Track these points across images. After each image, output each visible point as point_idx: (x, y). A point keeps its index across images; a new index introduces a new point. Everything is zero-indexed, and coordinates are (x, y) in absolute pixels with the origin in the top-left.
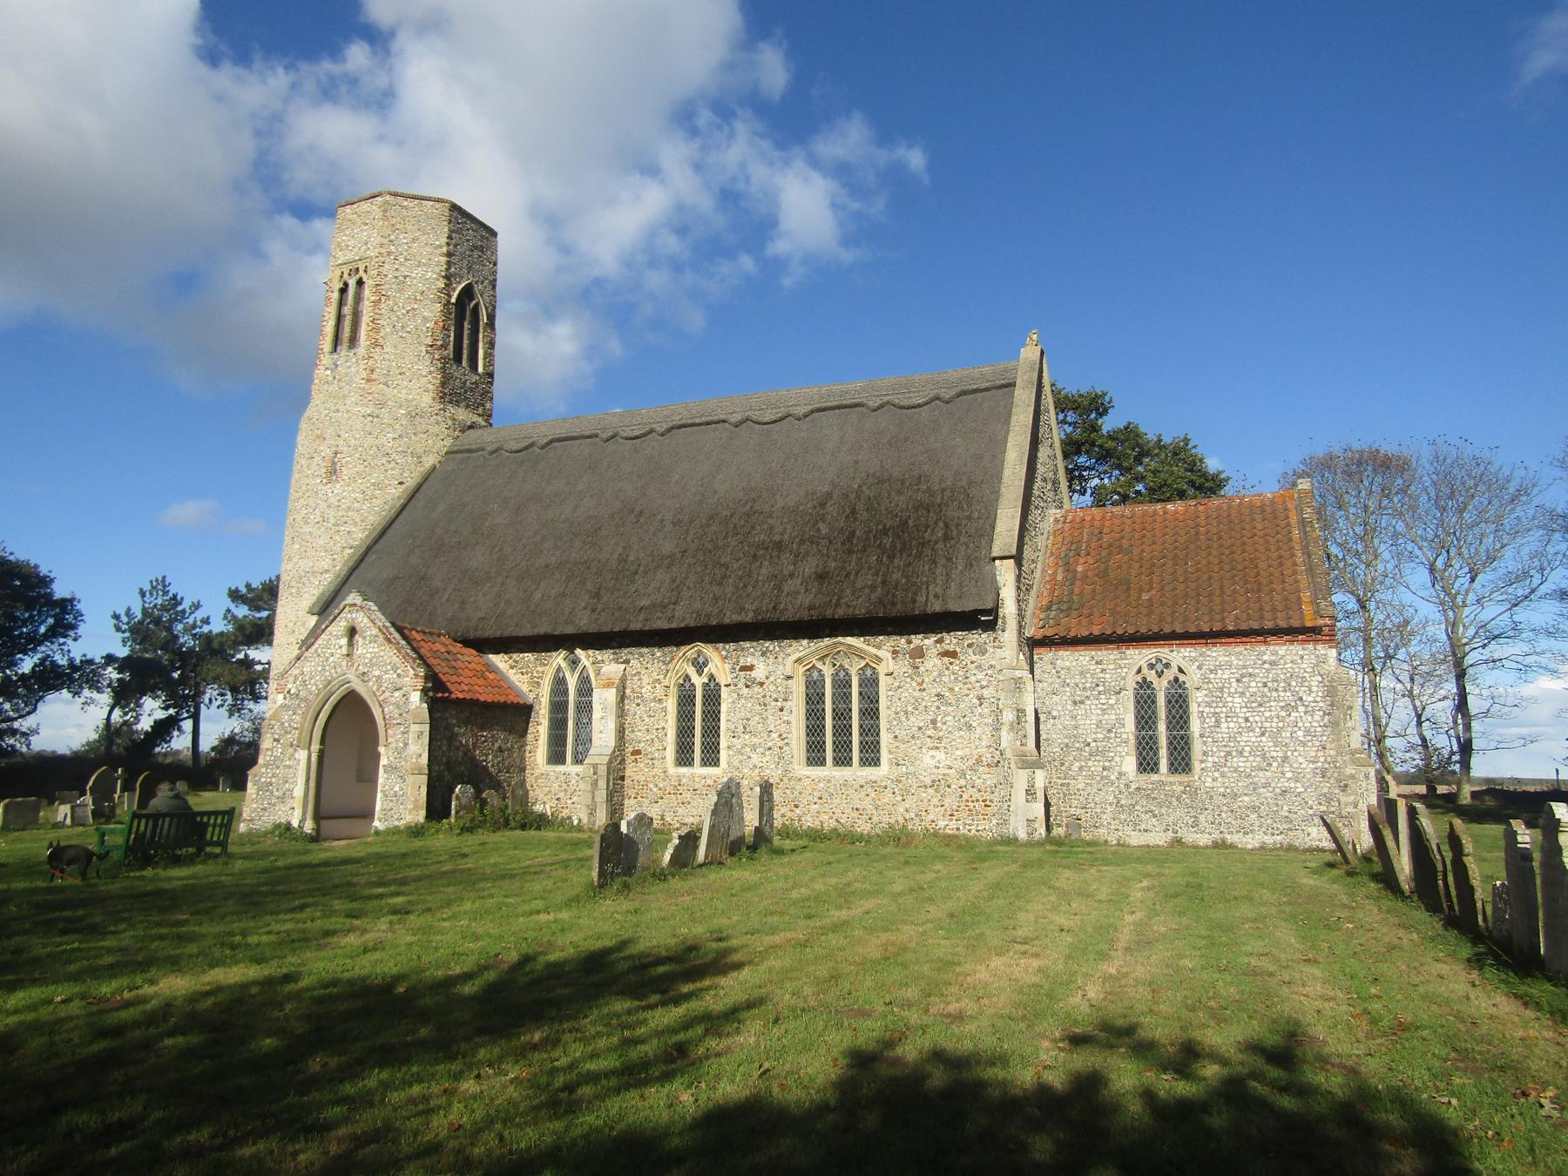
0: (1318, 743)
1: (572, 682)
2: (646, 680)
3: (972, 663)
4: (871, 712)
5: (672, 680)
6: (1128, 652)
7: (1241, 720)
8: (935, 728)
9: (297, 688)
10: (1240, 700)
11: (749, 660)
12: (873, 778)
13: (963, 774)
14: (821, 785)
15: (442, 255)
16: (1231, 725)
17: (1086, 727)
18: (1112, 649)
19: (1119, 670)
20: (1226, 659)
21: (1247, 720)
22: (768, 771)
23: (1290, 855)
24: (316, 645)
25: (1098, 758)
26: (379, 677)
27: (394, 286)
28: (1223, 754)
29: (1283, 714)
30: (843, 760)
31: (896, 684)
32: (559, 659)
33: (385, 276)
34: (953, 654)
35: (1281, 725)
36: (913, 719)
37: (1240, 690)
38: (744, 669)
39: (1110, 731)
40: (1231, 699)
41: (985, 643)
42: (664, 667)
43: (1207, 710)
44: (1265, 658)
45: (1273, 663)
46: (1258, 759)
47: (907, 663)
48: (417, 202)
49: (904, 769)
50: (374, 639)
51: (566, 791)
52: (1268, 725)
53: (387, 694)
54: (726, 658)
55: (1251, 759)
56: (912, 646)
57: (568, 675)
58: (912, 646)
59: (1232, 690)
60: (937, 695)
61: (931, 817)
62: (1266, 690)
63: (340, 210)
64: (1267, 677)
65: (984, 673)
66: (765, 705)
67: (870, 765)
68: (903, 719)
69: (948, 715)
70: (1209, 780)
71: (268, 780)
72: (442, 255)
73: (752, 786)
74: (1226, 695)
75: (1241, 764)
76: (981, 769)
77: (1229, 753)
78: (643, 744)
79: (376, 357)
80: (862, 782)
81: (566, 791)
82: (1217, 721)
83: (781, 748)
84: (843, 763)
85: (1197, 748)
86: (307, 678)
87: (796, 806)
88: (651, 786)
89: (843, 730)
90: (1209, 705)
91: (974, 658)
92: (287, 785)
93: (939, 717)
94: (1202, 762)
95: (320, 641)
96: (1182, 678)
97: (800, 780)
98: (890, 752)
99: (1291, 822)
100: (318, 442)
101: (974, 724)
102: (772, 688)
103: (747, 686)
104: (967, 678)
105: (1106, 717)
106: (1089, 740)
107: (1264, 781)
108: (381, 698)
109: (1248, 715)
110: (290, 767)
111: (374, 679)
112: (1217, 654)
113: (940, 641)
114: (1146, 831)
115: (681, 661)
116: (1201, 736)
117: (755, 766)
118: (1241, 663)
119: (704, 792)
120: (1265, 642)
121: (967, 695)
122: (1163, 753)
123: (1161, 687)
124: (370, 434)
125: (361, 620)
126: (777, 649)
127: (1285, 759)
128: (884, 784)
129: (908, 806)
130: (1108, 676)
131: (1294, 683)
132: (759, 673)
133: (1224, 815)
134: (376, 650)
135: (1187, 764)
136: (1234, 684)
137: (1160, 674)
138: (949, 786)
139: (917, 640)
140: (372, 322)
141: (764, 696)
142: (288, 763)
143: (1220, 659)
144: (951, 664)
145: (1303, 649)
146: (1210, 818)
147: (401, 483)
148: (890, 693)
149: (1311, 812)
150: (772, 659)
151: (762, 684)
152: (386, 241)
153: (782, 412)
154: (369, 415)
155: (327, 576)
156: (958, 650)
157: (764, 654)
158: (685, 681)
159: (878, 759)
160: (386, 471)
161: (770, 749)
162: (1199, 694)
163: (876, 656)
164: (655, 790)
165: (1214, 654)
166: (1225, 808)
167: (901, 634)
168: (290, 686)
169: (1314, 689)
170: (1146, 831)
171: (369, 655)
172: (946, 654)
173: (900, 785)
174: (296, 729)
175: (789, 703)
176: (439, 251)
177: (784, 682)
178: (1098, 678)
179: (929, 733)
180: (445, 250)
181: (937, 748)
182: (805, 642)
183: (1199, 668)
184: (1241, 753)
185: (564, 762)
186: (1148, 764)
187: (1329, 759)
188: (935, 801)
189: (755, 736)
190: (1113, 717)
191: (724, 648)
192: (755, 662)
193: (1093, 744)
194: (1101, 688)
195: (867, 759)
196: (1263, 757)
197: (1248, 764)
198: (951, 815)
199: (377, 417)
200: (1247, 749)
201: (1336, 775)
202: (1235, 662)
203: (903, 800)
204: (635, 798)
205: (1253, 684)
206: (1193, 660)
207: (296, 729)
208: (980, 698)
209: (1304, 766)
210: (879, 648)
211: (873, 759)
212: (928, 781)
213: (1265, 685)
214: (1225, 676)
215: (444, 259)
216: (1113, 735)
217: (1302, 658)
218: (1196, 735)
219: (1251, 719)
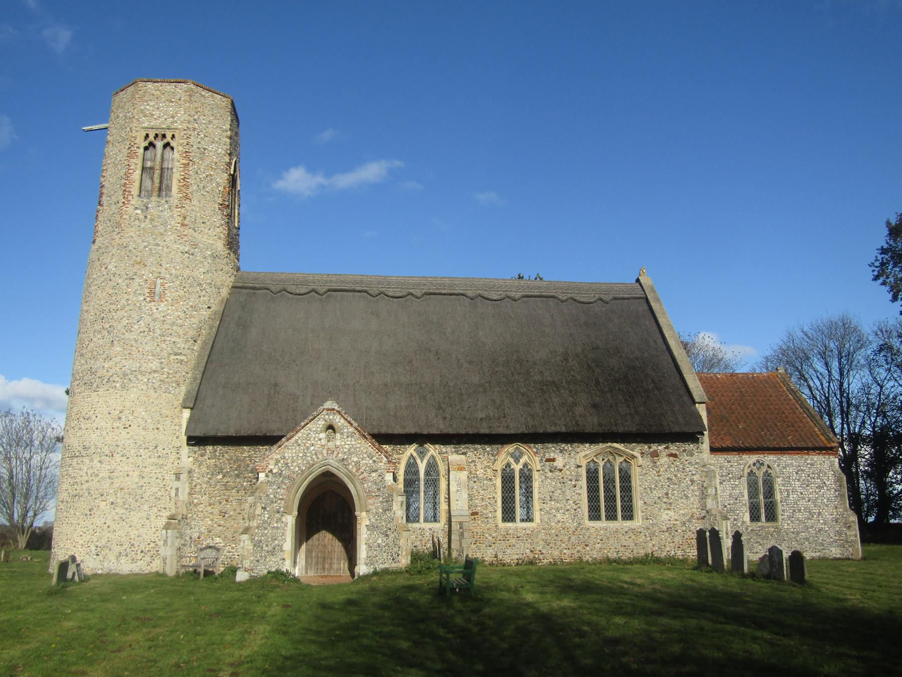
0: (833, 505)
1: (422, 467)
2: (479, 466)
3: (686, 461)
4: (627, 489)
5: (499, 466)
6: (743, 457)
7: (799, 494)
8: (668, 498)
10: (798, 483)
11: (552, 455)
12: (633, 527)
13: (684, 524)
14: (602, 532)
15: (227, 137)
16: (795, 496)
17: (724, 497)
18: (735, 454)
19: (739, 466)
20: (791, 462)
21: (801, 493)
22: (567, 524)
23: (848, 562)
24: (296, 437)
25: (731, 514)
26: (357, 463)
27: (197, 155)
28: (791, 511)
29: (817, 490)
30: (611, 517)
31: (644, 472)
32: (411, 450)
33: (192, 146)
34: (675, 456)
35: (817, 496)
36: (655, 492)
37: (798, 478)
38: (548, 460)
39: (736, 499)
40: (793, 482)
41: (693, 450)
42: (492, 458)
43: (783, 488)
44: (808, 461)
45: (812, 465)
46: (808, 514)
47: (649, 460)
48: (210, 93)
49: (651, 521)
50: (351, 435)
51: (421, 540)
52: (811, 496)
53: (365, 474)
54: (536, 453)
55: (805, 513)
56: (651, 450)
57: (418, 461)
58: (651, 450)
59: (794, 478)
60: (668, 479)
61: (668, 549)
62: (809, 478)
63: (220, 102)
64: (809, 472)
65: (693, 467)
66: (564, 483)
67: (627, 519)
68: (649, 492)
69: (675, 490)
70: (786, 525)
71: (260, 538)
72: (227, 137)
73: (557, 534)
74: (791, 481)
75: (800, 516)
76: (694, 521)
77: (794, 511)
78: (479, 508)
79: (187, 208)
80: (627, 529)
81: (421, 540)
82: (788, 494)
83: (575, 510)
84: (611, 518)
85: (780, 508)
86: (289, 461)
87: (587, 545)
88: (487, 535)
89: (610, 499)
90: (783, 485)
91: (687, 458)
92: (277, 542)
93: (670, 491)
94: (782, 515)
95: (299, 434)
96: (770, 471)
97: (588, 529)
98: (642, 512)
99: (823, 545)
100: (137, 267)
101: (690, 495)
102: (568, 473)
103: (551, 471)
104: (684, 469)
105: (734, 491)
106: (726, 504)
107: (811, 524)
108: (361, 477)
109: (802, 491)
110: (277, 528)
111: (353, 464)
112: (786, 459)
113: (667, 448)
114: (757, 553)
115: (505, 454)
116: (781, 502)
117: (559, 521)
118: (797, 464)
119: (525, 539)
120: (808, 454)
121: (684, 479)
122: (763, 510)
123: (760, 474)
124: (188, 267)
125: (339, 421)
126: (570, 449)
127: (819, 513)
128: (640, 530)
129: (654, 543)
130: (734, 469)
131: (821, 475)
132: (559, 463)
133: (793, 543)
134: (354, 443)
135: (774, 517)
136: (795, 475)
137: (758, 469)
138: (677, 531)
139: (654, 447)
140: (183, 179)
141: (563, 478)
142: (275, 525)
143: (788, 461)
144: (675, 461)
145: (825, 458)
146: (787, 545)
147: (209, 308)
148: (641, 477)
149: (832, 540)
150: (567, 455)
151: (561, 470)
152: (192, 119)
153: (503, 295)
154: (186, 252)
155: (156, 375)
156: (678, 453)
157: (561, 451)
158: (506, 467)
159: (632, 516)
160: (200, 297)
161: (568, 510)
162: (779, 480)
163: (633, 455)
164: (490, 538)
165: (785, 459)
166: (793, 539)
167: (645, 443)
168: (271, 467)
169: (830, 478)
170: (757, 553)
171: (347, 446)
172: (671, 455)
173: (649, 531)
174: (282, 499)
175: (580, 482)
176: (225, 134)
177: (576, 470)
178: (729, 470)
179: (665, 500)
180: (229, 133)
181: (669, 509)
182: (587, 445)
183: (778, 466)
184: (800, 511)
185: (418, 521)
186: (755, 517)
187: (839, 513)
188: (669, 539)
189: (558, 502)
190: (738, 491)
191: (535, 447)
192: (556, 456)
193: (728, 506)
194: (731, 476)
195: (626, 516)
196: (810, 512)
197: (803, 516)
198: (679, 547)
199: (192, 254)
200: (802, 508)
201: (844, 521)
202: (794, 464)
203: (651, 540)
204: (475, 544)
205: (803, 475)
206: (775, 462)
207: (282, 499)
208: (692, 481)
209: (828, 517)
210: (632, 450)
211: (629, 516)
212: (665, 528)
213: (809, 476)
214: (791, 471)
215: (228, 141)
216: (738, 501)
217: (824, 462)
218: (779, 501)
219: (803, 493)
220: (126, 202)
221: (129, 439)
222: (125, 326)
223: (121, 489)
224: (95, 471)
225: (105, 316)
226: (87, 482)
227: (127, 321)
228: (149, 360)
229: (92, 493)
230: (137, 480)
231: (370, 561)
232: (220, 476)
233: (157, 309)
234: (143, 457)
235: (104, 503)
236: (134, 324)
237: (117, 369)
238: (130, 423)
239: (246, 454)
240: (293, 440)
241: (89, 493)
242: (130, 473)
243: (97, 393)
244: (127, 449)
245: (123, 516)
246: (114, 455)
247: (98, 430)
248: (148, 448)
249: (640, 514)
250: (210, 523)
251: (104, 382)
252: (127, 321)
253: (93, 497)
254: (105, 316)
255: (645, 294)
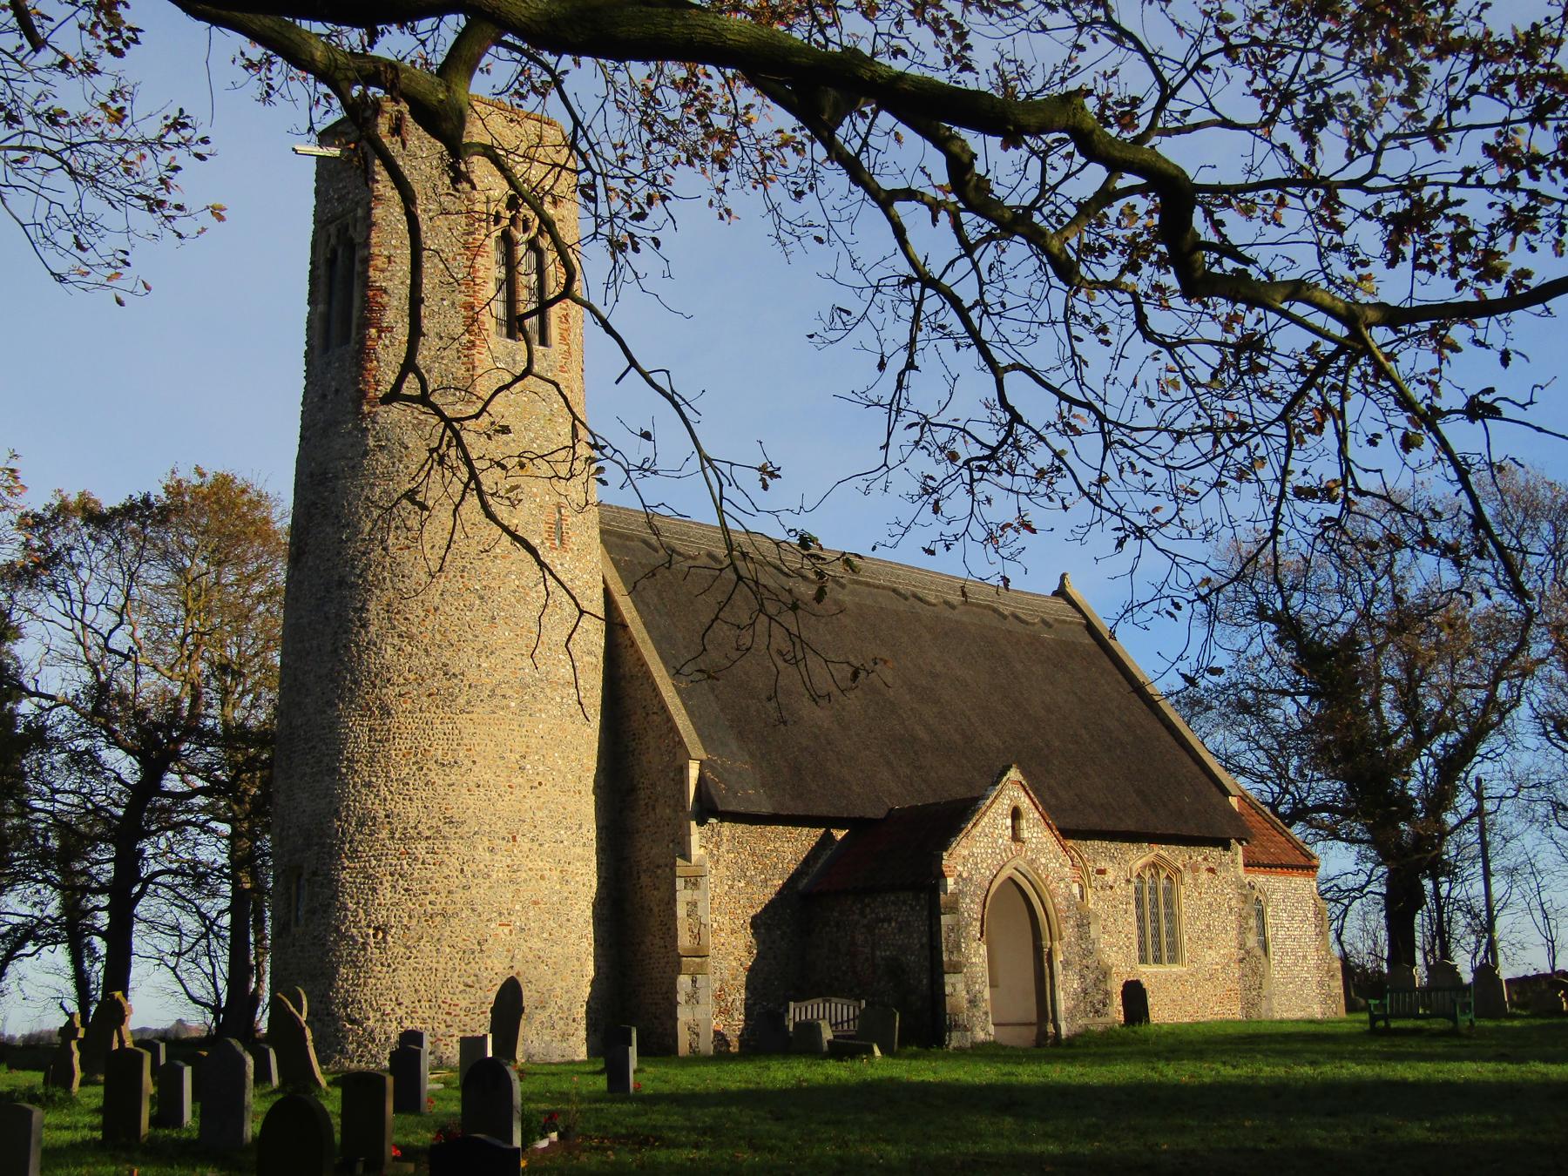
9: (970, 873)
26: (1046, 866)
30: (1158, 960)
95: (986, 819)
132: (1109, 878)
220: (478, 342)
221: (539, 809)
222: (514, 591)
223: (536, 903)
224: (482, 866)
225: (469, 566)
226: (466, 888)
227: (517, 582)
228: (560, 661)
229: (480, 909)
230: (558, 887)
231: (1071, 1016)
232: (742, 884)
233: (562, 565)
234: (566, 843)
235: (506, 930)
236: (531, 589)
237: (506, 672)
238: (539, 779)
239: (771, 846)
240: (979, 828)
241: (473, 910)
242: (547, 874)
243: (470, 716)
244: (539, 828)
245: (542, 954)
246: (518, 839)
247: (481, 789)
248: (571, 829)
249: (1187, 955)
250: (734, 964)
251: (484, 695)
252: (517, 582)
253: (485, 917)
254: (469, 566)
255: (1085, 616)
